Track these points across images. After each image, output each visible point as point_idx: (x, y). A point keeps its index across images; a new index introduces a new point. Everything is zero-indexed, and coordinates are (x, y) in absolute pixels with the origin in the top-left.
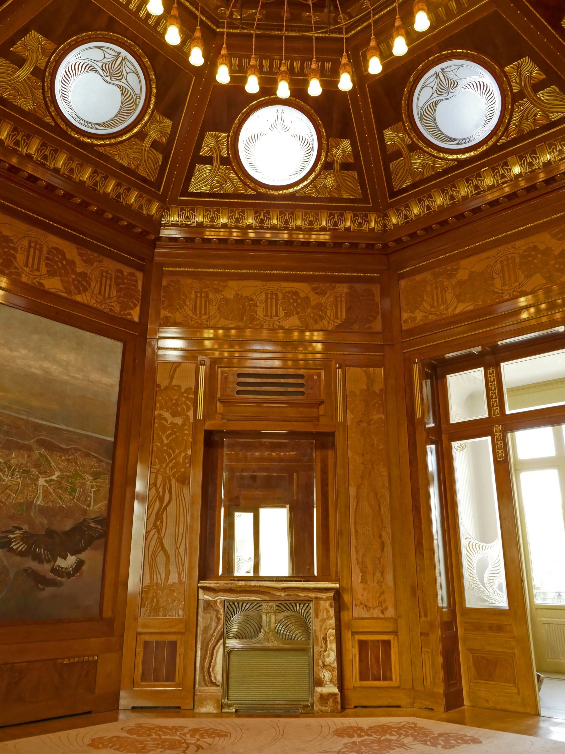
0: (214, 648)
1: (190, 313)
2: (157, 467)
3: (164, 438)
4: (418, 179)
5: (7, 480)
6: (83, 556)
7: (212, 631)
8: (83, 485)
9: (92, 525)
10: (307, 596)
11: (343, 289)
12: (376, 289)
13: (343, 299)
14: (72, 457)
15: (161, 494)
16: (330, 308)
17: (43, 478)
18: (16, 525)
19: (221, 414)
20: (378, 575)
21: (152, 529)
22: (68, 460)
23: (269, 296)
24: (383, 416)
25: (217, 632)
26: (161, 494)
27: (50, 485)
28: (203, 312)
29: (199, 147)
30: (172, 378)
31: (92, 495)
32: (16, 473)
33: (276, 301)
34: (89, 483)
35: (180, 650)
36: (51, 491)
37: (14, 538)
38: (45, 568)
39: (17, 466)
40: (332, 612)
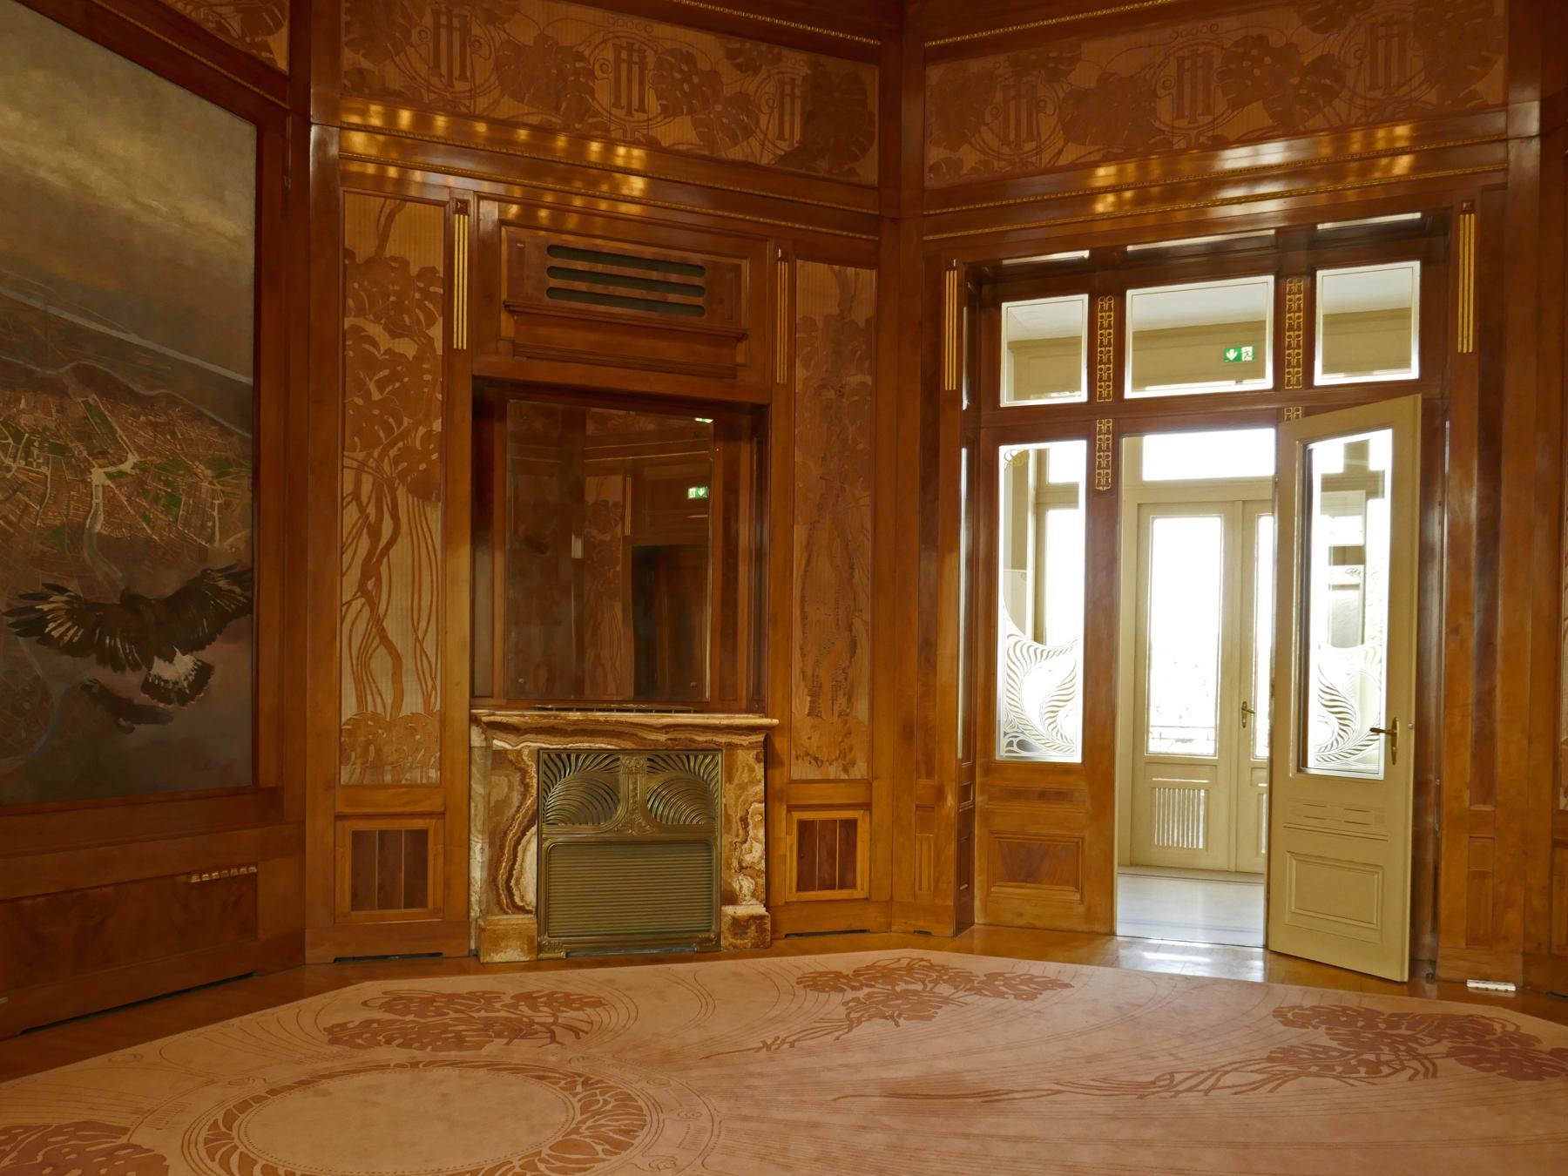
0: (518, 842)
1: (423, 69)
2: (360, 455)
3: (372, 386)
5: (14, 467)
6: (207, 655)
7: (512, 811)
8: (194, 489)
9: (222, 583)
10: (711, 741)
11: (796, 64)
12: (871, 78)
13: (798, 93)
14: (161, 419)
15: (372, 518)
16: (766, 109)
17: (101, 466)
18: (51, 581)
19: (512, 342)
20: (842, 701)
21: (355, 598)
22: (155, 425)
23: (624, 55)
24: (869, 380)
25: (523, 811)
26: (372, 518)
27: (119, 486)
28: (457, 73)
30: (383, 238)
31: (215, 513)
32: (36, 452)
33: (642, 71)
34: (205, 485)
35: (434, 848)
36: (123, 499)
37: (50, 611)
38: (128, 682)
39: (33, 432)
40: (759, 771)
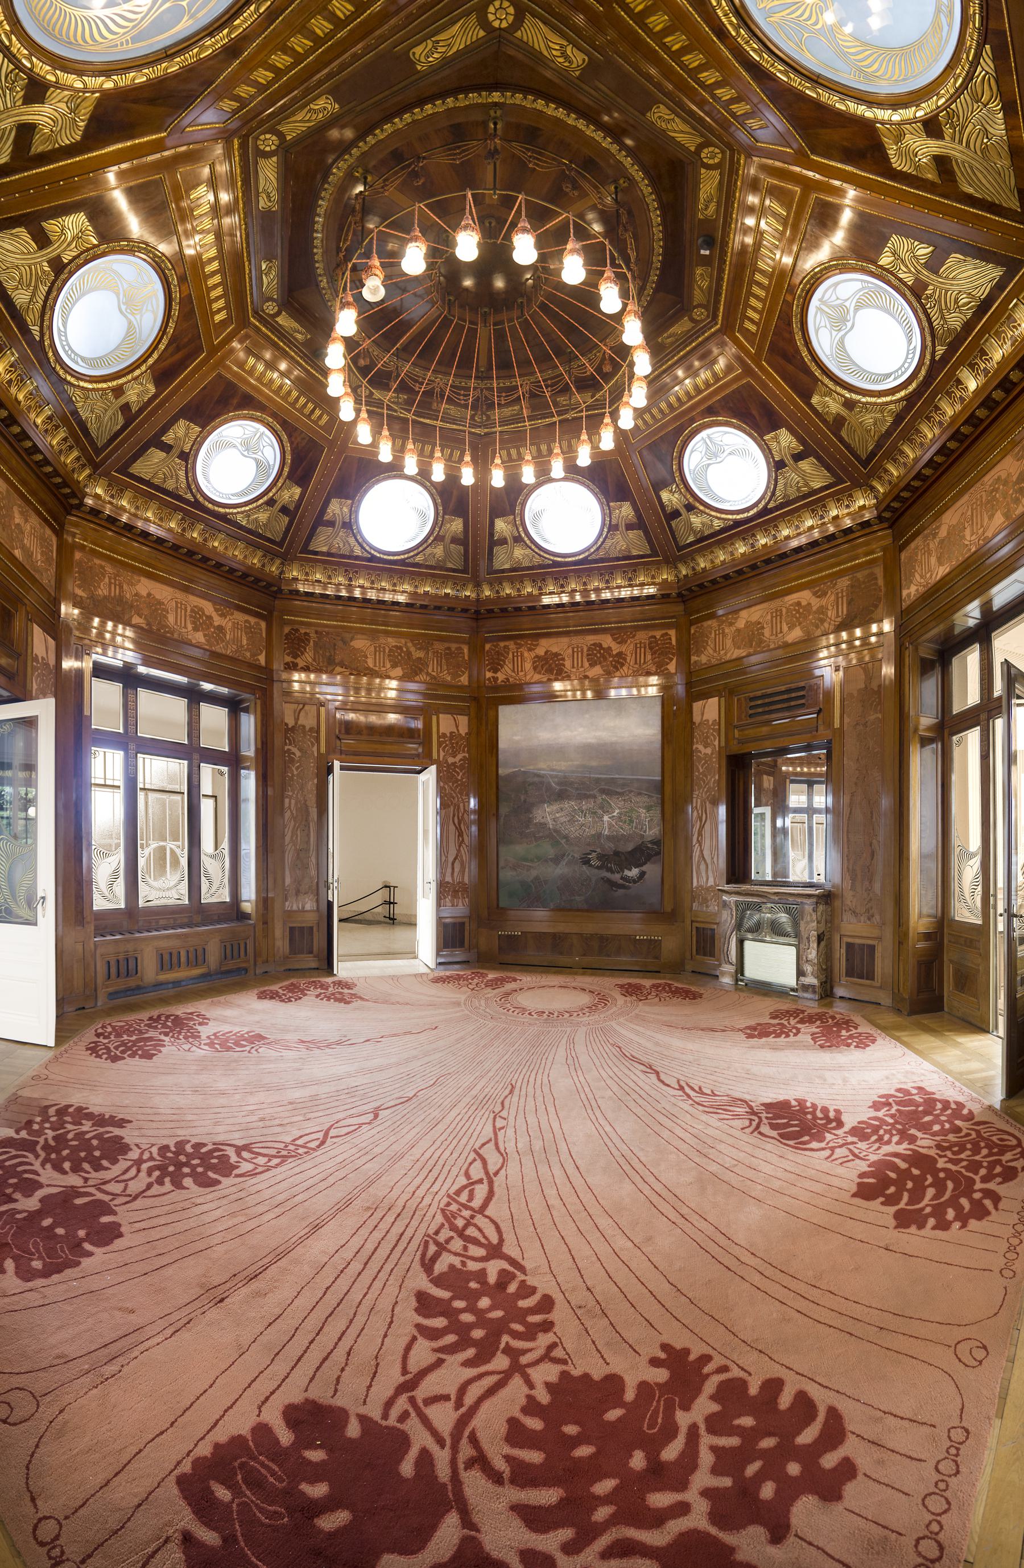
38: (616, 877)
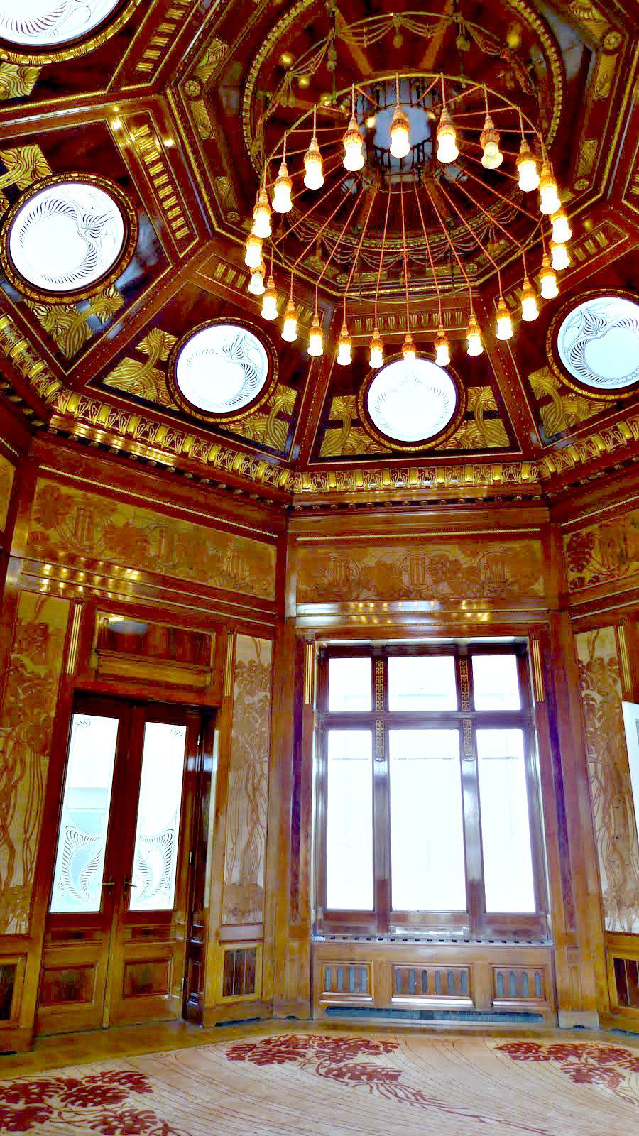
2: (9, 730)
4: (347, 453)
29: (139, 338)
30: (38, 612)
